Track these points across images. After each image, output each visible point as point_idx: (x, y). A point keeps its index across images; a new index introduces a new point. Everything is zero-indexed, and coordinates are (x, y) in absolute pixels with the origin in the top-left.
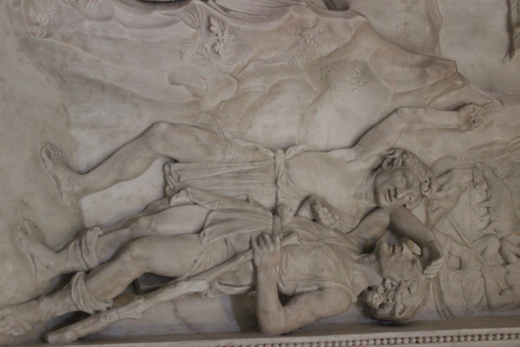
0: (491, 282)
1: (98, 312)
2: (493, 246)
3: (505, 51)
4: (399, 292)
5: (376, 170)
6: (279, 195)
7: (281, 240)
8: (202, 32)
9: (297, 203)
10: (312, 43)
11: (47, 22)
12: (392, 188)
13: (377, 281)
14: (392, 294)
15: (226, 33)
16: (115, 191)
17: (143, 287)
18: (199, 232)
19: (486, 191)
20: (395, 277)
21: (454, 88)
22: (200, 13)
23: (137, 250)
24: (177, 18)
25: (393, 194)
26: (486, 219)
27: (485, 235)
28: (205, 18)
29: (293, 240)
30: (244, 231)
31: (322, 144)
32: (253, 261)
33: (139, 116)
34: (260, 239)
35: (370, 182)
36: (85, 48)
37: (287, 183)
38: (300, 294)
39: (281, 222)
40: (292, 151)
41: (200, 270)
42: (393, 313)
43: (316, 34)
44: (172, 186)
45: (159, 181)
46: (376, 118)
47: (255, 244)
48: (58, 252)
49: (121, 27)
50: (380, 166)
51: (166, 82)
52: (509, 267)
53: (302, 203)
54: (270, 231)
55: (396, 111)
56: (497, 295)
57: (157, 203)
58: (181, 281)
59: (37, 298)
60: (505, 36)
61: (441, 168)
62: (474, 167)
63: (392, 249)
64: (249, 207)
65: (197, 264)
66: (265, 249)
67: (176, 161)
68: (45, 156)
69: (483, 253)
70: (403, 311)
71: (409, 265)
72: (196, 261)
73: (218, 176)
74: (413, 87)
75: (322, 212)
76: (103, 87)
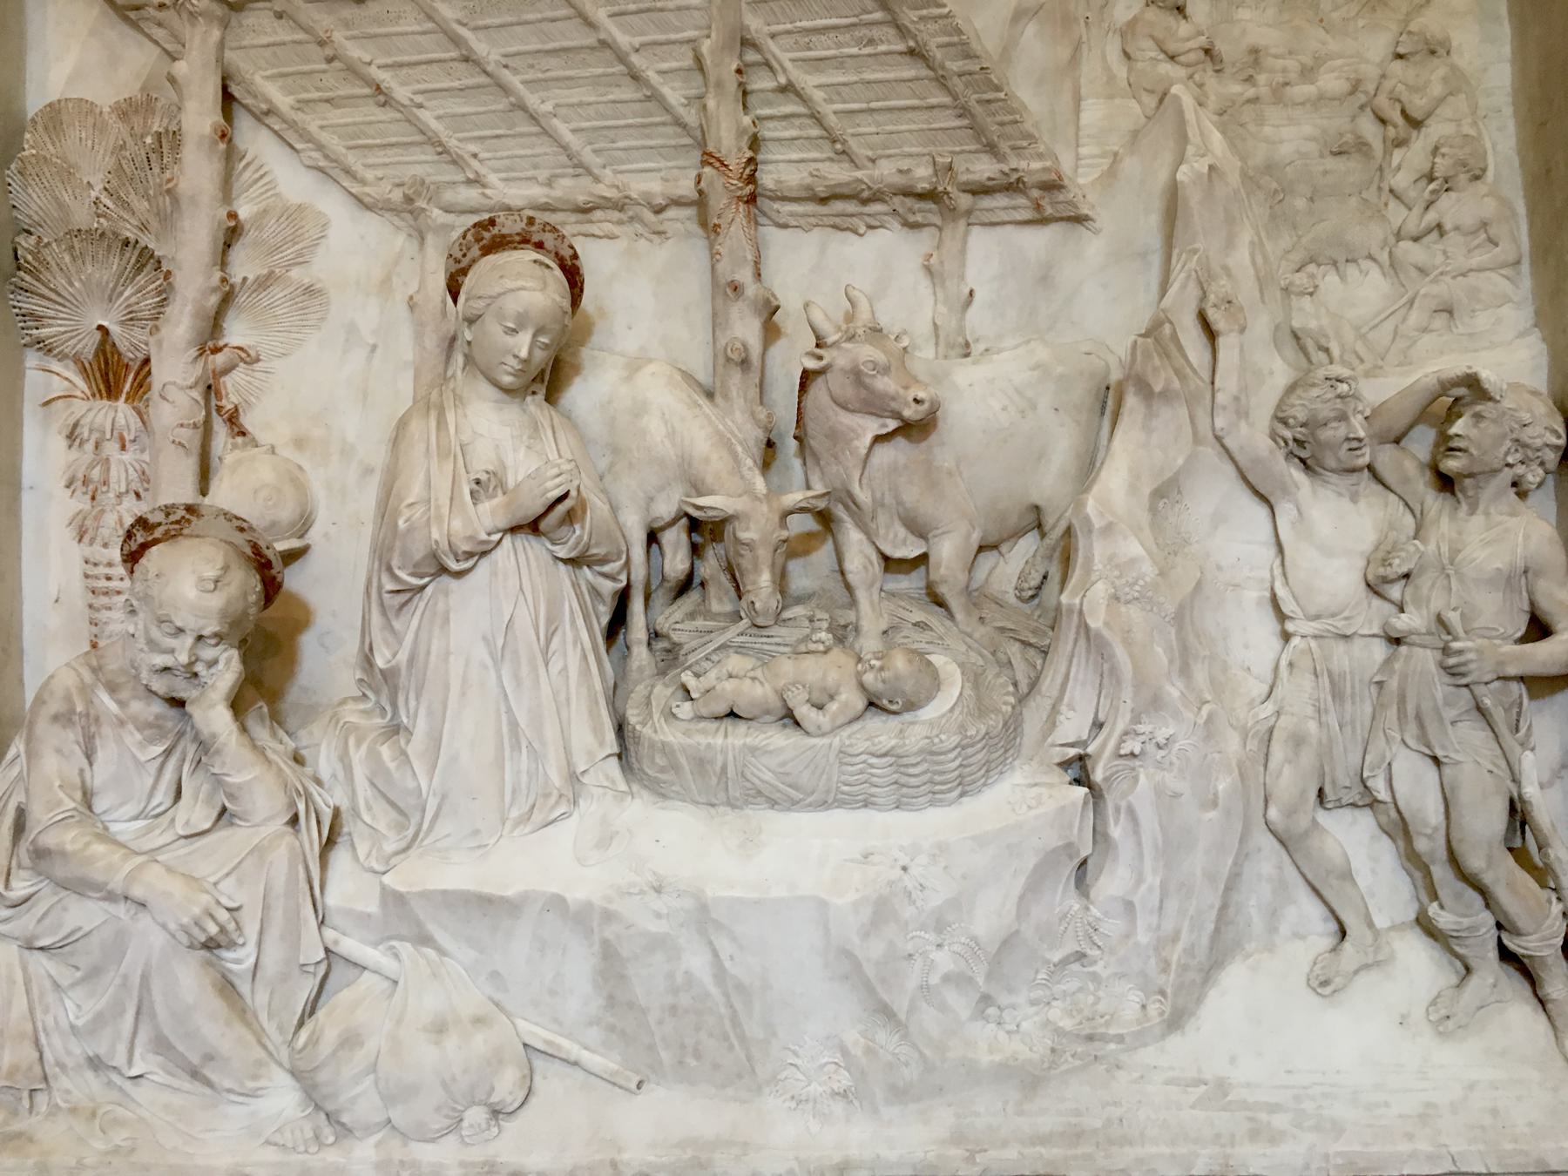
0: (1477, 259)
2: (1411, 252)
3: (1080, 229)
4: (1530, 441)
6: (1366, 632)
7: (1456, 639)
8: (1141, 766)
10: (1137, 588)
11: (1139, 993)
12: (1346, 446)
14: (1530, 453)
15: (1141, 728)
16: (1363, 880)
17: (1518, 843)
18: (1436, 760)
19: (1319, 265)
20: (1504, 449)
21: (1174, 337)
22: (1114, 769)
23: (1475, 862)
24: (1123, 804)
25: (1355, 444)
27: (1392, 265)
29: (1453, 618)
30: (1439, 695)
33: (1259, 850)
34: (1452, 672)
35: (1334, 478)
36: (1175, 939)
37: (1346, 618)
38: (1532, 603)
39: (1419, 634)
40: (1288, 606)
41: (1503, 764)
43: (1124, 581)
44: (1357, 797)
45: (1347, 813)
46: (1229, 469)
47: (1464, 681)
48: (1468, 969)
49: (1144, 887)
50: (1303, 461)
51: (1212, 814)
52: (1448, 226)
54: (1438, 655)
55: (1218, 439)
56: (1498, 249)
57: (1383, 819)
58: (1520, 796)
63: (1458, 453)
64: (1393, 684)
65: (1495, 770)
66: (1472, 666)
68: (1327, 990)
70: (1555, 432)
71: (1482, 425)
72: (1490, 772)
73: (1341, 727)
74: (1183, 412)
76: (1224, 907)
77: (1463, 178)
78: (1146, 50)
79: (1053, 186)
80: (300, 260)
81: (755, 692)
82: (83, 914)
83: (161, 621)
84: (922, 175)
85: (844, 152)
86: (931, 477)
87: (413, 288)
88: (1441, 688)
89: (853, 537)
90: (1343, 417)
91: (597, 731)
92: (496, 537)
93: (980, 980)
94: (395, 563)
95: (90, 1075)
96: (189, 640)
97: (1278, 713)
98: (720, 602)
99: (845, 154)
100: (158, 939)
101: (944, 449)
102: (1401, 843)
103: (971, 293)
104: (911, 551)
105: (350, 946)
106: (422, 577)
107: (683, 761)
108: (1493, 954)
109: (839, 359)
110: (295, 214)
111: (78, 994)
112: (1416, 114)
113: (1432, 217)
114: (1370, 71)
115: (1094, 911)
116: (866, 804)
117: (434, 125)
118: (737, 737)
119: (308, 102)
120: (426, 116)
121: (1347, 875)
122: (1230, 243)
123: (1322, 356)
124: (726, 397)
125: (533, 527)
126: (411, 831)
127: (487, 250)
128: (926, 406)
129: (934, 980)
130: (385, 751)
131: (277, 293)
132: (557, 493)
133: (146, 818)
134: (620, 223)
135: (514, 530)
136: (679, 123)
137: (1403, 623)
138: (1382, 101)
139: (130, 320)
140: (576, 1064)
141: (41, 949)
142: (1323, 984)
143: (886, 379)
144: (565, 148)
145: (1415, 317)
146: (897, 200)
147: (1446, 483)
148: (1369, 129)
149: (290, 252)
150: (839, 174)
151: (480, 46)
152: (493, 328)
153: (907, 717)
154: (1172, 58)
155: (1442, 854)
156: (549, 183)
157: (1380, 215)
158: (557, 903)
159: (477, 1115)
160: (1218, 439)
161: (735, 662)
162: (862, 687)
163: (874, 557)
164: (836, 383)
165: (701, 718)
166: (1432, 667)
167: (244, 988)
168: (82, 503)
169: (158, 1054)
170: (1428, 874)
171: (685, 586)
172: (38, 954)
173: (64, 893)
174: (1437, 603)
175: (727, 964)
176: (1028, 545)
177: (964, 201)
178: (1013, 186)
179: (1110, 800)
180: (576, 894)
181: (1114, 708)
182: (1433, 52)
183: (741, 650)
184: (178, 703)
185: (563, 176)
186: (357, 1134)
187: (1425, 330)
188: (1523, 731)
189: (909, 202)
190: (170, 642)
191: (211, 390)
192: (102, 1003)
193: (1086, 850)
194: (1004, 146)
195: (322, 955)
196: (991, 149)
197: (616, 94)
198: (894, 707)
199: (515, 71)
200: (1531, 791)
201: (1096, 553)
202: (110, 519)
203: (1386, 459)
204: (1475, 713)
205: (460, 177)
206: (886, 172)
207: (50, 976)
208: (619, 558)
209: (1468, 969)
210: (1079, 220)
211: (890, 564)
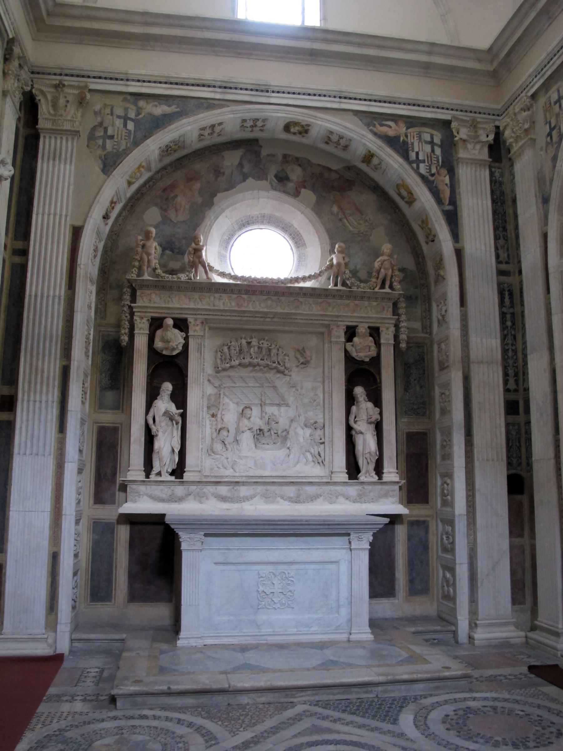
81: (265, 442)
82: (218, 456)
84: (278, 403)
89: (272, 431)
98: (262, 435)
109: (272, 417)
142: (305, 464)
150: (271, 402)
151: (244, 391)
178: (285, 404)
184: (223, 442)
201: (290, 433)
206: (275, 402)
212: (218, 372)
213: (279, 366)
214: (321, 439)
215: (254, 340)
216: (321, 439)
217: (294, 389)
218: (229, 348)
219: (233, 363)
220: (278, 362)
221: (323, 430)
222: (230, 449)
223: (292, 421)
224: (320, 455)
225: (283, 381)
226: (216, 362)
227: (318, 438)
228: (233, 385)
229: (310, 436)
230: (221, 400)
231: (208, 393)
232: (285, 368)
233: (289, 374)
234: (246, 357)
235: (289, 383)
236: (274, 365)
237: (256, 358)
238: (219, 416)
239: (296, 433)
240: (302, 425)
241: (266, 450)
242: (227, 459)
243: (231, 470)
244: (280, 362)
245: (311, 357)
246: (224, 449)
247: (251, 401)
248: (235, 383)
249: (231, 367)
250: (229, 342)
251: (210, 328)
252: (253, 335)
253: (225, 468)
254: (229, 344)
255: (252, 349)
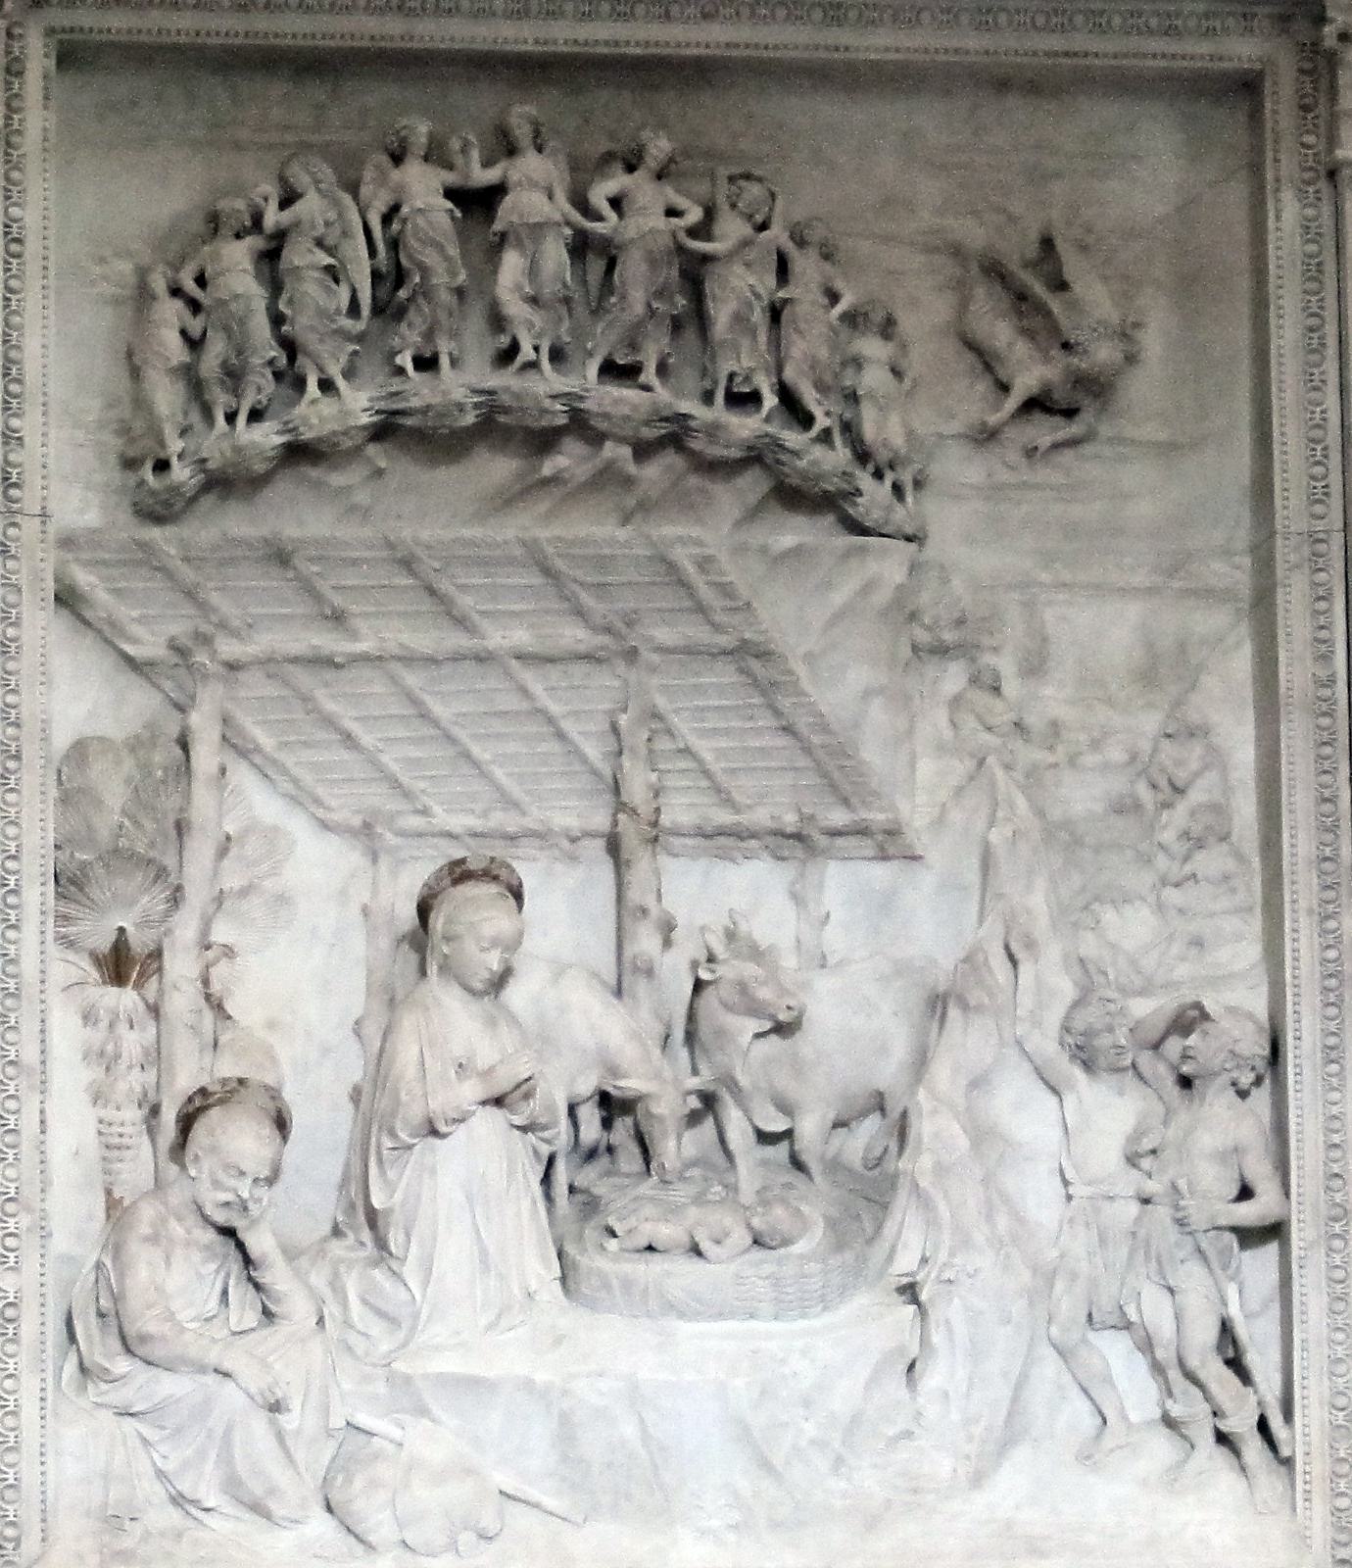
0: (1218, 907)
1: (1259, 1403)
2: (1172, 895)
3: (915, 865)
5: (1088, 1066)
9: (1135, 1172)
13: (1225, 1078)
16: (1122, 1384)
17: (1231, 1354)
18: (1171, 1291)
23: (1193, 1362)
26: (1138, 903)
28: (941, 1286)
29: (1182, 1184)
31: (1056, 1133)
32: (1206, 1231)
34: (1181, 1223)
42: (1263, 1057)
46: (1027, 1066)
47: (1188, 1229)
48: (1192, 1447)
50: (1084, 1063)
51: (1009, 1328)
52: (1200, 876)
53: (1134, 1165)
54: (1172, 1211)
55: (1019, 1043)
59: (1243, 1469)
60: (895, 865)
61: (1077, 969)
62: (1075, 925)
64: (1142, 1233)
67: (1090, 1315)
69: (1181, 911)
70: (1261, 1046)
75: (1147, 1144)
76: (1015, 1399)
77: (1212, 840)
78: (970, 723)
79: (893, 832)
80: (274, 872)
81: (665, 1232)
82: (169, 1385)
83: (227, 1167)
84: (790, 820)
85: (728, 800)
86: (798, 1067)
87: (366, 897)
88: (1173, 1234)
90: (1110, 1029)
91: (544, 1259)
92: (474, 1108)
93: (837, 1445)
94: (398, 1125)
95: (171, 1508)
96: (249, 1181)
97: (1062, 1256)
98: (629, 1159)
99: (728, 801)
100: (239, 1399)
101: (804, 1044)
102: (1149, 1357)
103: (828, 915)
104: (778, 1125)
105: (363, 1419)
106: (415, 1138)
107: (615, 1283)
108: (1209, 1438)
110: (272, 835)
111: (163, 1449)
112: (1179, 784)
113: (1188, 869)
114: (1146, 746)
115: (921, 1400)
116: (752, 1316)
117: (394, 767)
118: (656, 1265)
119: (286, 744)
120: (385, 758)
121: (1108, 1380)
122: (1029, 888)
123: (1101, 979)
124: (634, 997)
125: (498, 1101)
126: (401, 1335)
127: (458, 880)
128: (796, 1013)
129: (803, 1443)
130: (379, 1275)
131: (255, 900)
132: (526, 1076)
133: (199, 1321)
134: (542, 848)
135: (484, 1103)
136: (595, 772)
137: (1152, 1187)
138: (1154, 772)
139: (144, 923)
140: (537, 1506)
141: (131, 1415)
142: (1086, 1457)
143: (765, 989)
144: (498, 788)
145: (1175, 950)
146: (770, 840)
147: (1186, 1082)
148: (1143, 791)
149: (265, 867)
150: (724, 817)
151: (438, 709)
152: (470, 947)
153: (782, 1251)
154: (989, 729)
155: (1175, 1361)
156: (485, 814)
157: (1147, 861)
158: (528, 1385)
159: (467, 1538)
160: (1019, 1043)
161: (649, 1210)
162: (749, 1226)
163: (750, 1130)
164: (726, 991)
165: (623, 1250)
166: (1168, 1220)
167: (289, 1443)
168: (98, 1073)
169: (226, 1493)
170: (1166, 1381)
171: (591, 1154)
172: (129, 1419)
173: (154, 1371)
174: (1171, 1173)
175: (651, 1430)
176: (872, 1124)
177: (823, 841)
178: (862, 831)
179: (934, 1315)
180: (541, 1377)
181: (936, 1247)
182: (1192, 735)
183: (652, 1199)
184: (229, 1232)
185: (495, 809)
186: (380, 1549)
187: (1183, 959)
188: (1234, 1265)
189: (780, 840)
190: (232, 1182)
191: (206, 982)
192: (189, 1452)
193: (914, 1350)
194: (854, 800)
195: (344, 1423)
196: (846, 802)
197: (543, 748)
198: (774, 1243)
199: (463, 726)
200: (1234, 1310)
201: (924, 1128)
202: (122, 1086)
203: (1145, 1060)
204: (1198, 1255)
205: (410, 807)
206: (760, 817)
207: (140, 1435)
208: (556, 1127)
209: (1192, 1447)
210: (915, 858)
211: (764, 1138)
212: (157, 511)
213: (793, 438)
214: (1245, 1193)
215: (531, 166)
216: (1245, 1193)
217: (953, 678)
218: (270, 257)
219: (315, 415)
220: (789, 399)
221: (1261, 1097)
222: (297, 1307)
223: (938, 1005)
224: (1236, 1364)
225: (839, 597)
226: (141, 403)
227: (1213, 1183)
228: (327, 641)
229: (1132, 1160)
230: (202, 800)
231: (62, 740)
232: (863, 456)
233: (900, 516)
234: (444, 347)
235: (904, 611)
236: (745, 426)
237: (557, 355)
238: (181, 966)
239: (982, 1135)
240: (1047, 1044)
241: (671, 1308)
242: (276, 1407)
243: (320, 1525)
244: (810, 397)
245: (1126, 334)
246: (243, 1311)
247: (512, 804)
248: (337, 618)
249: (298, 453)
250: (271, 190)
251: (71, 56)
252: (521, 116)
253: (258, 1508)
254: (272, 218)
255: (512, 263)
